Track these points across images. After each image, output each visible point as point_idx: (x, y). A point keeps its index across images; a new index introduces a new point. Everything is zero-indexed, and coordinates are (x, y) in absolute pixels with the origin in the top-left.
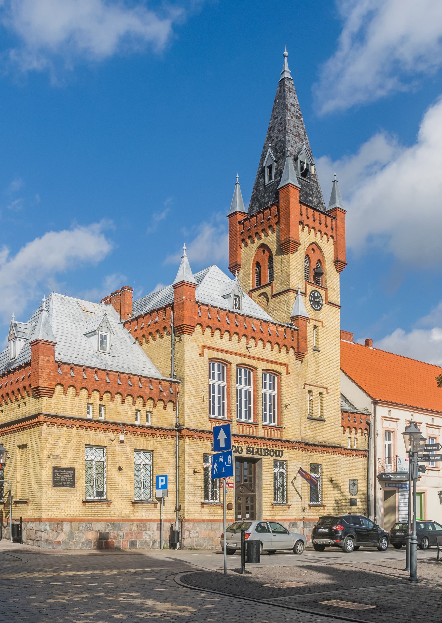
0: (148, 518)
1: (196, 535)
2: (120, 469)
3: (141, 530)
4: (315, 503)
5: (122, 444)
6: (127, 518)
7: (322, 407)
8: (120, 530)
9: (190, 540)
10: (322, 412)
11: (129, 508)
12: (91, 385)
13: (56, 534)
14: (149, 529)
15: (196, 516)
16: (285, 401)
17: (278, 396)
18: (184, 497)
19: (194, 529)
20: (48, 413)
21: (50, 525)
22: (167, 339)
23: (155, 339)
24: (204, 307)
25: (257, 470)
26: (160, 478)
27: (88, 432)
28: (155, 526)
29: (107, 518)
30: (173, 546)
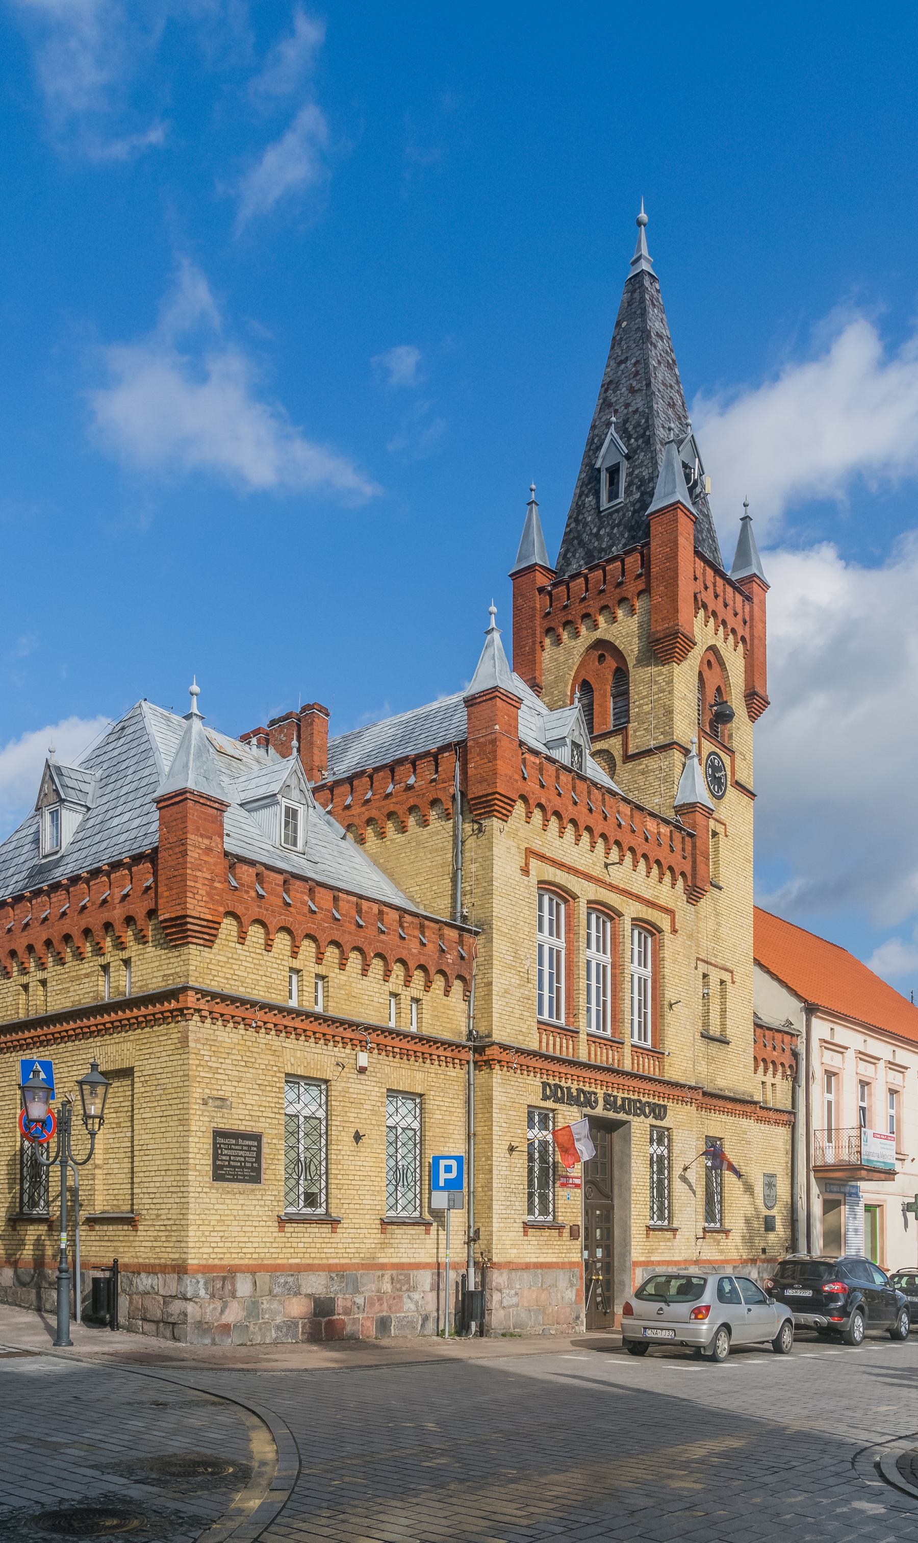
0: (412, 1260)
1: (515, 1300)
2: (358, 1137)
3: (400, 1290)
5: (362, 1077)
7: (723, 1012)
8: (357, 1291)
9: (502, 1313)
10: (723, 1025)
11: (374, 1236)
12: (300, 923)
13: (219, 1304)
14: (415, 1288)
15: (512, 1255)
16: (670, 995)
17: (654, 981)
18: (490, 1208)
19: (510, 1287)
21: (206, 1284)
22: (439, 830)
23: (403, 829)
25: (617, 1148)
26: (443, 1163)
27: (291, 1043)
28: (426, 1279)
29: (331, 1261)
30: (462, 1328)
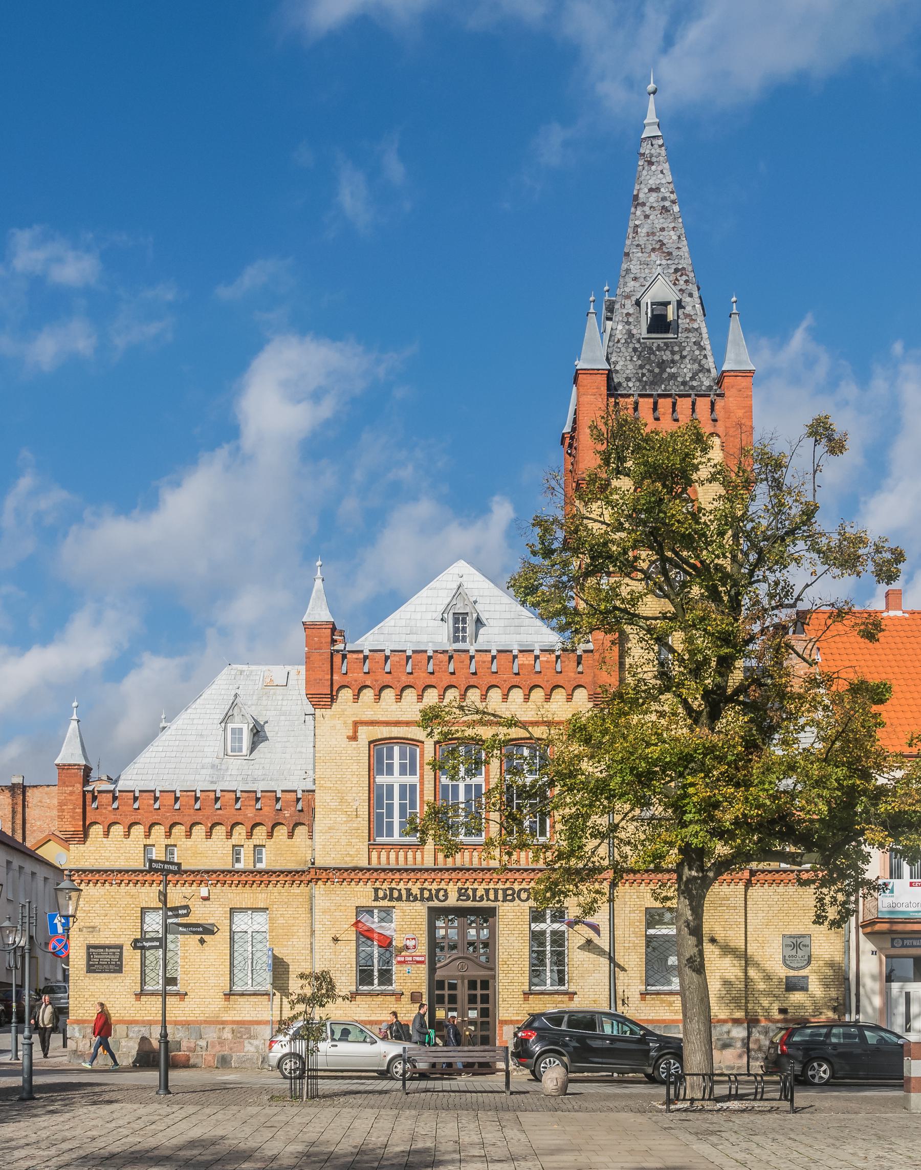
0: (255, 1019)
3: (241, 1037)
4: (666, 988)
5: (207, 902)
6: (215, 1019)
11: (220, 1002)
12: (147, 818)
14: (255, 1037)
20: (80, 867)
21: (80, 1030)
24: (355, 656)
29: (179, 1019)
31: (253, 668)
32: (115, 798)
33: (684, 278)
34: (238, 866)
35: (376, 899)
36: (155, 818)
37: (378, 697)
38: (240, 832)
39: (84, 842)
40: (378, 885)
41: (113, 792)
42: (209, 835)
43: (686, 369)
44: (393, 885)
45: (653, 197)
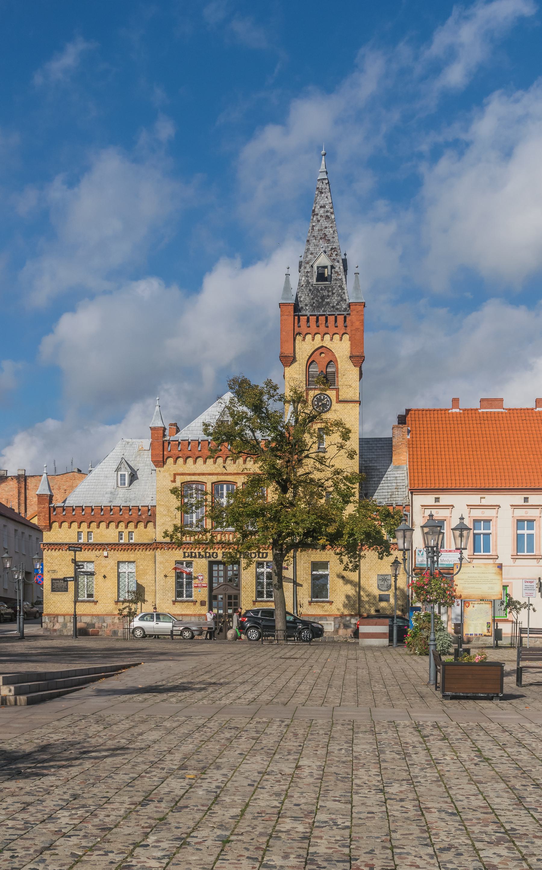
2: (105, 577)
31: (134, 440)
32: (64, 510)
33: (336, 253)
34: (121, 541)
35: (184, 557)
36: (83, 519)
37: (185, 462)
38: (122, 525)
39: (50, 530)
40: (185, 550)
41: (63, 507)
42: (108, 527)
43: (335, 299)
44: (192, 551)
45: (322, 211)
